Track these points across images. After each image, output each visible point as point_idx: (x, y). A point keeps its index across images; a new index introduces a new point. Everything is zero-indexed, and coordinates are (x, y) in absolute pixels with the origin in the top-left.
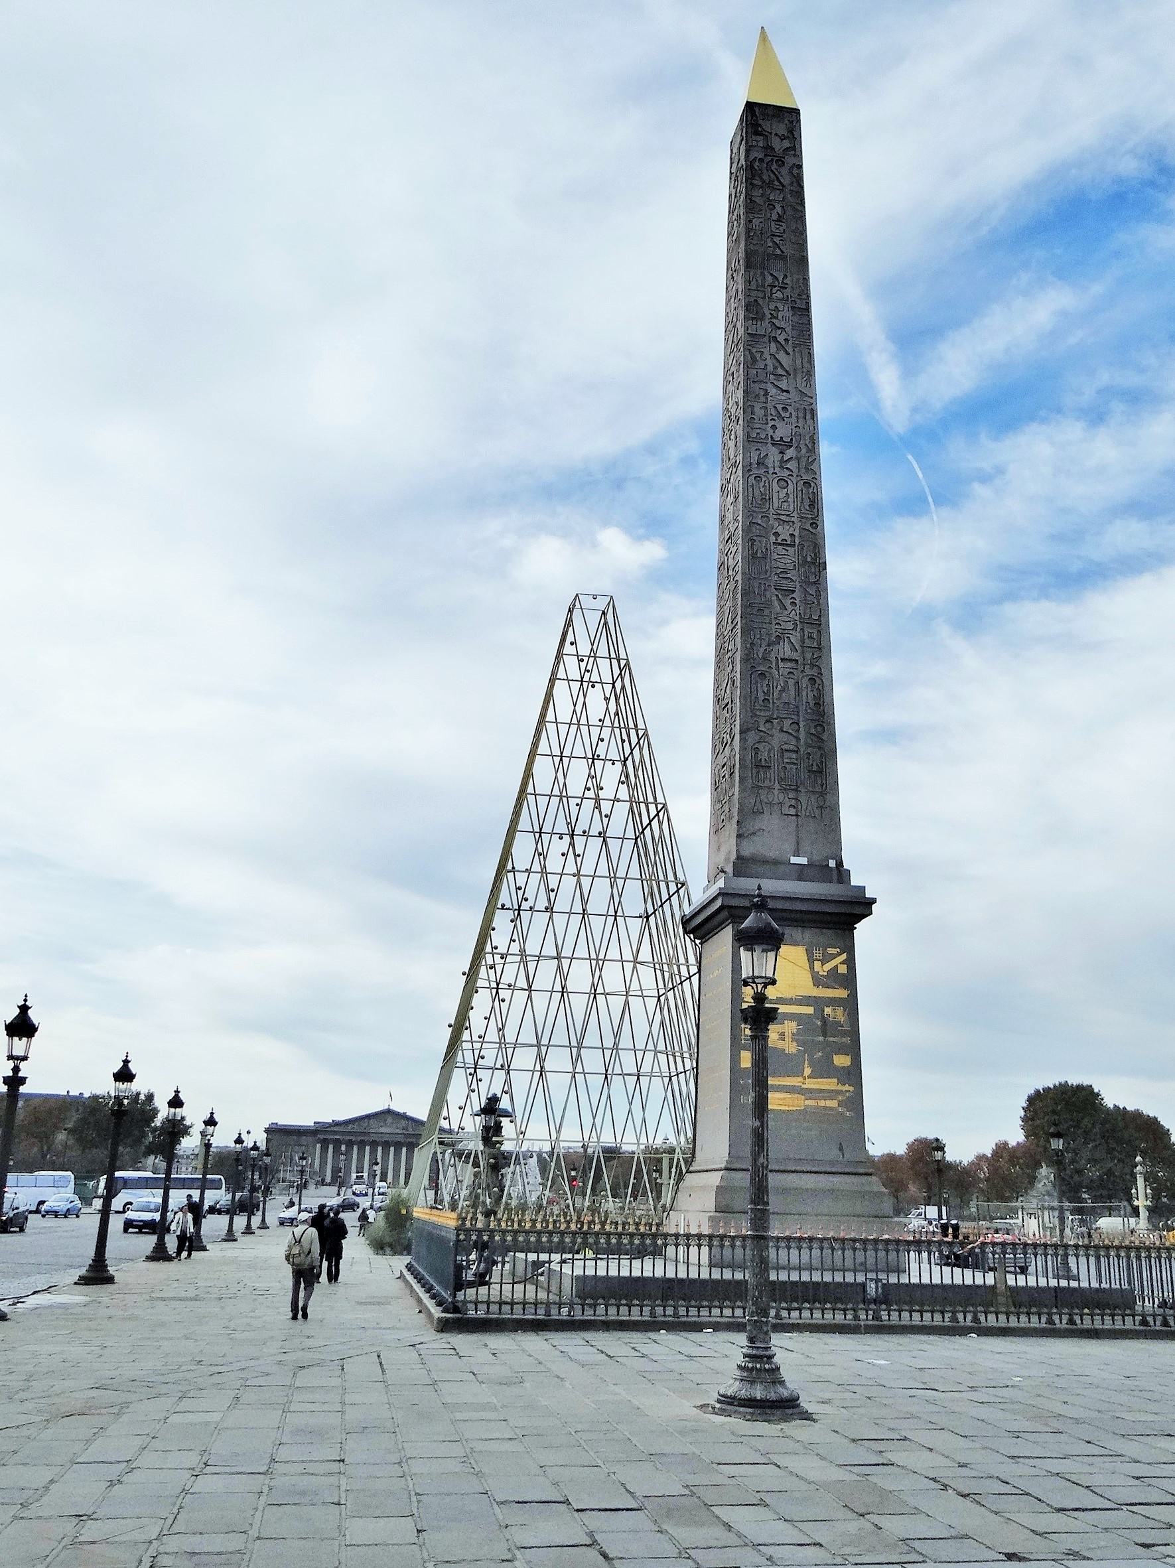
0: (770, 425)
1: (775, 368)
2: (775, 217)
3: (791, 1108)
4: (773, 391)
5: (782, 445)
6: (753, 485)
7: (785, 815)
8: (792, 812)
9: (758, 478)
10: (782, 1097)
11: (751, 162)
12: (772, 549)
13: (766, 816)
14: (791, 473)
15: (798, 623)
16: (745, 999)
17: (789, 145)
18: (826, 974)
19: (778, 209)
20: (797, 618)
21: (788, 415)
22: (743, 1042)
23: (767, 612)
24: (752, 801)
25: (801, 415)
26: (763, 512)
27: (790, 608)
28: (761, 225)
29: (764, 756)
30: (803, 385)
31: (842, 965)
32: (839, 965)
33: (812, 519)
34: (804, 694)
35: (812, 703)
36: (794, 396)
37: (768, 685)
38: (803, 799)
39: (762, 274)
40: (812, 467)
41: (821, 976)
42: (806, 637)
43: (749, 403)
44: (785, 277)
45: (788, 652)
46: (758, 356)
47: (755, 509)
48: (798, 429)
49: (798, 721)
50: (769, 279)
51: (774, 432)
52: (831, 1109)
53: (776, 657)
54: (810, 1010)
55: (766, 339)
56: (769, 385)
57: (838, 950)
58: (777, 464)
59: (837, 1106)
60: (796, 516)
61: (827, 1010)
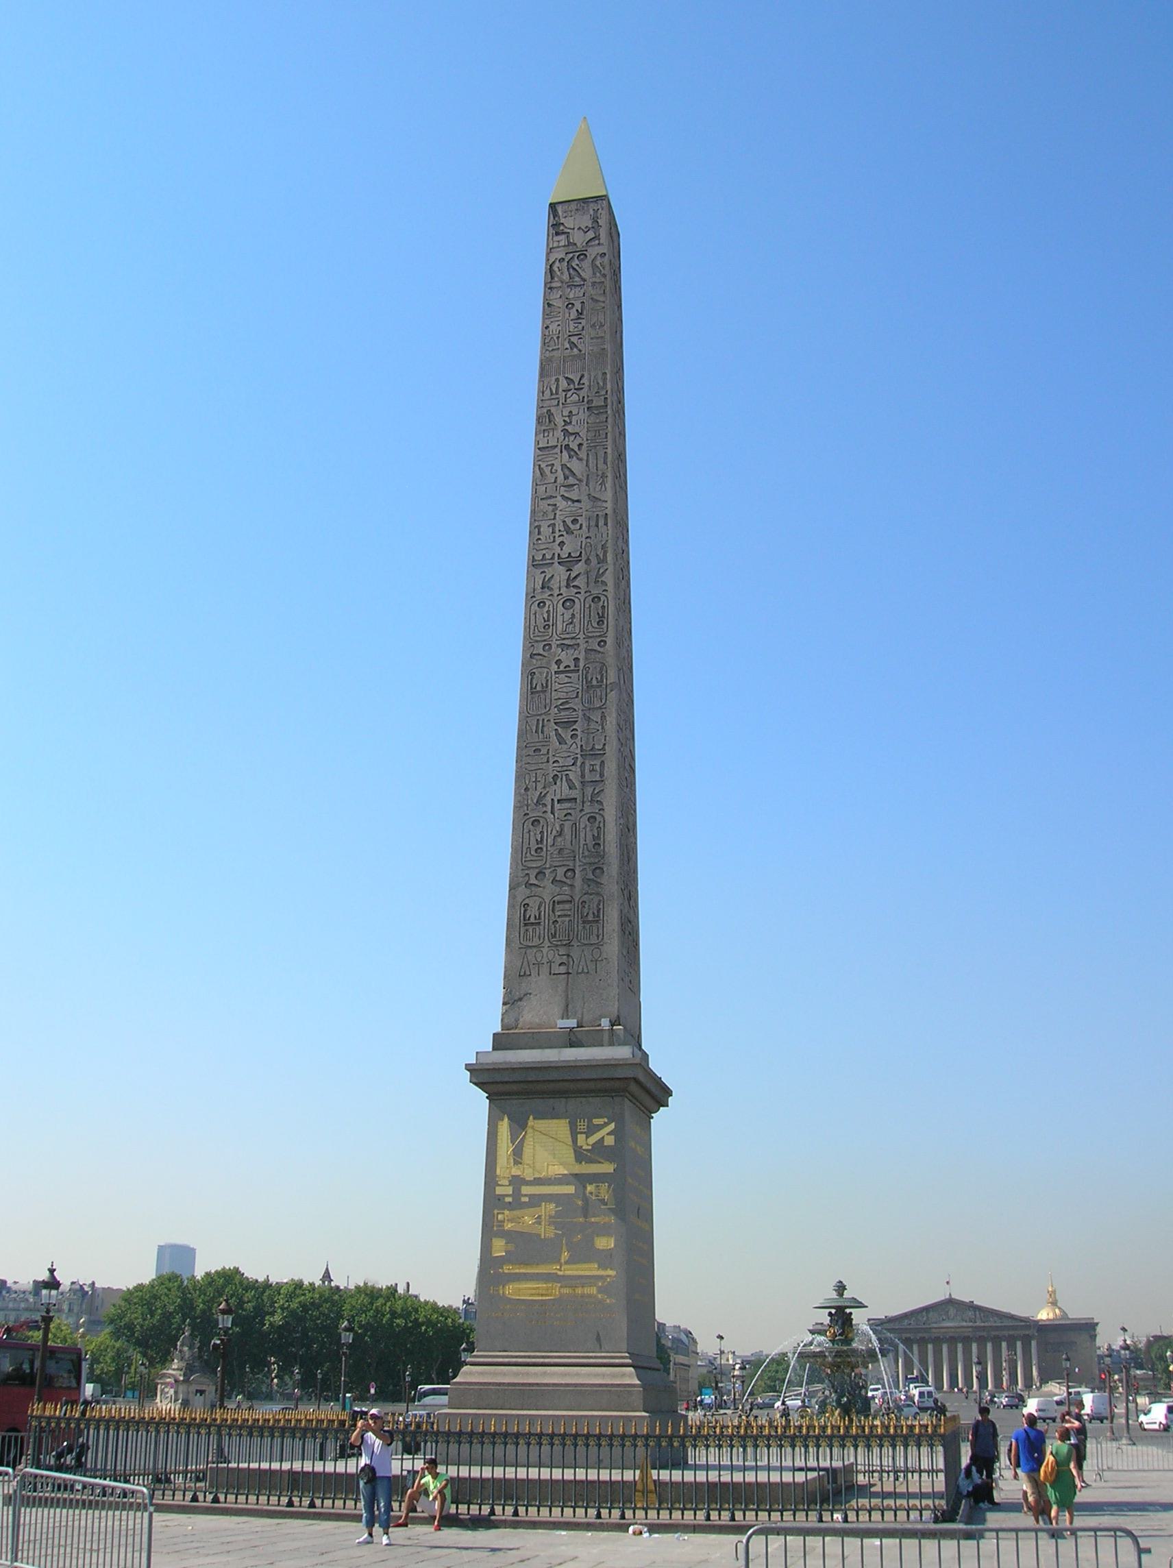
0: (557, 542)
1: (566, 478)
2: (574, 314)
3: (544, 1298)
4: (562, 504)
5: (568, 562)
6: (535, 614)
7: (554, 974)
8: (563, 969)
9: (541, 604)
11: (551, 266)
12: (553, 678)
13: (533, 978)
14: (579, 590)
15: (579, 756)
17: (594, 236)
18: (590, 1147)
19: (578, 306)
20: (578, 751)
21: (578, 526)
22: (495, 1229)
23: (544, 751)
24: (519, 964)
25: (593, 523)
26: (545, 641)
27: (569, 741)
28: (560, 328)
29: (533, 912)
30: (597, 490)
31: (609, 1137)
32: (605, 1138)
33: (600, 636)
34: (582, 835)
35: (590, 846)
36: (586, 504)
37: (542, 832)
38: (575, 953)
39: (557, 380)
40: (603, 579)
42: (587, 771)
43: (537, 524)
44: (582, 376)
45: (566, 792)
46: (547, 470)
47: (538, 639)
48: (588, 540)
49: (574, 866)
50: (564, 384)
51: (562, 549)
52: (590, 1296)
53: (552, 800)
54: (570, 1189)
55: (557, 450)
56: (559, 498)
57: (606, 1120)
58: (564, 583)
60: (581, 636)
61: (589, 1188)
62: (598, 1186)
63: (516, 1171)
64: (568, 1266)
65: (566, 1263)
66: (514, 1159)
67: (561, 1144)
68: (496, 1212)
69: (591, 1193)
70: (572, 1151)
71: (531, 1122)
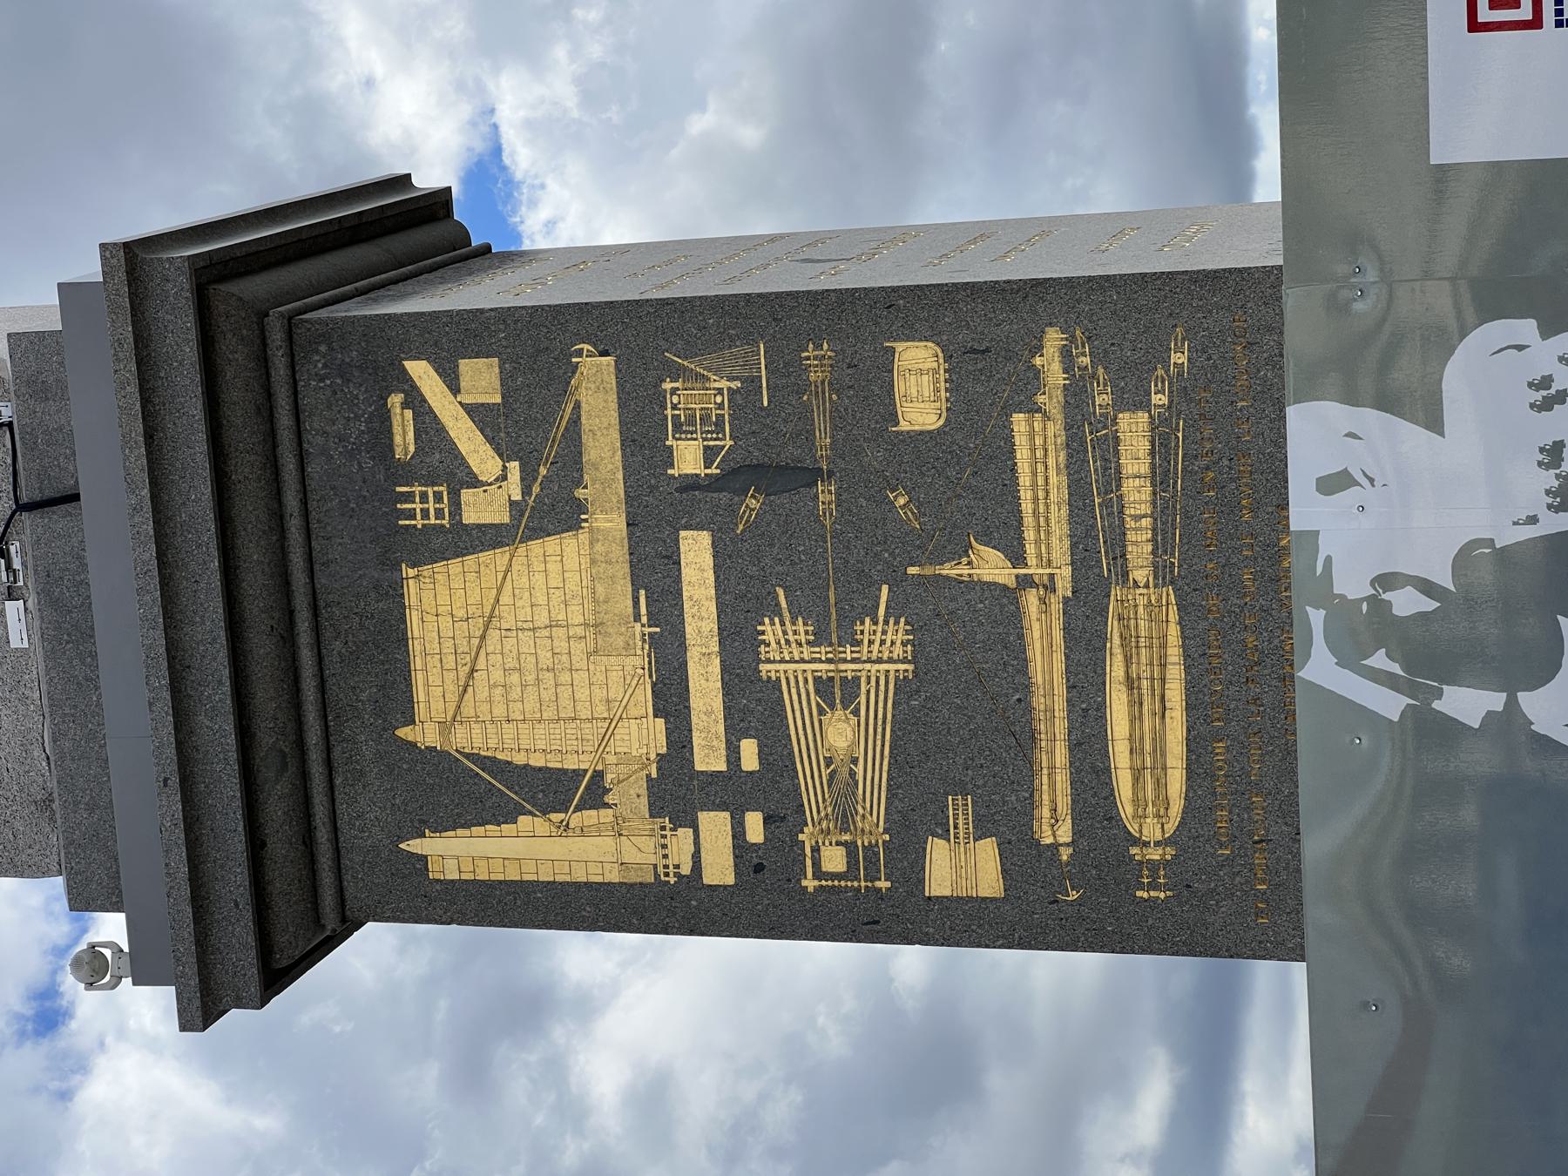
3: (1174, 653)
10: (1124, 697)
16: (686, 870)
18: (514, 466)
22: (883, 884)
32: (468, 400)
41: (526, 491)
52: (1160, 445)
57: (395, 400)
59: (1143, 417)
61: (688, 459)
62: (678, 426)
63: (631, 795)
64: (1032, 560)
65: (1017, 558)
66: (578, 809)
67: (506, 598)
68: (810, 883)
69: (709, 455)
70: (535, 546)
71: (423, 734)
